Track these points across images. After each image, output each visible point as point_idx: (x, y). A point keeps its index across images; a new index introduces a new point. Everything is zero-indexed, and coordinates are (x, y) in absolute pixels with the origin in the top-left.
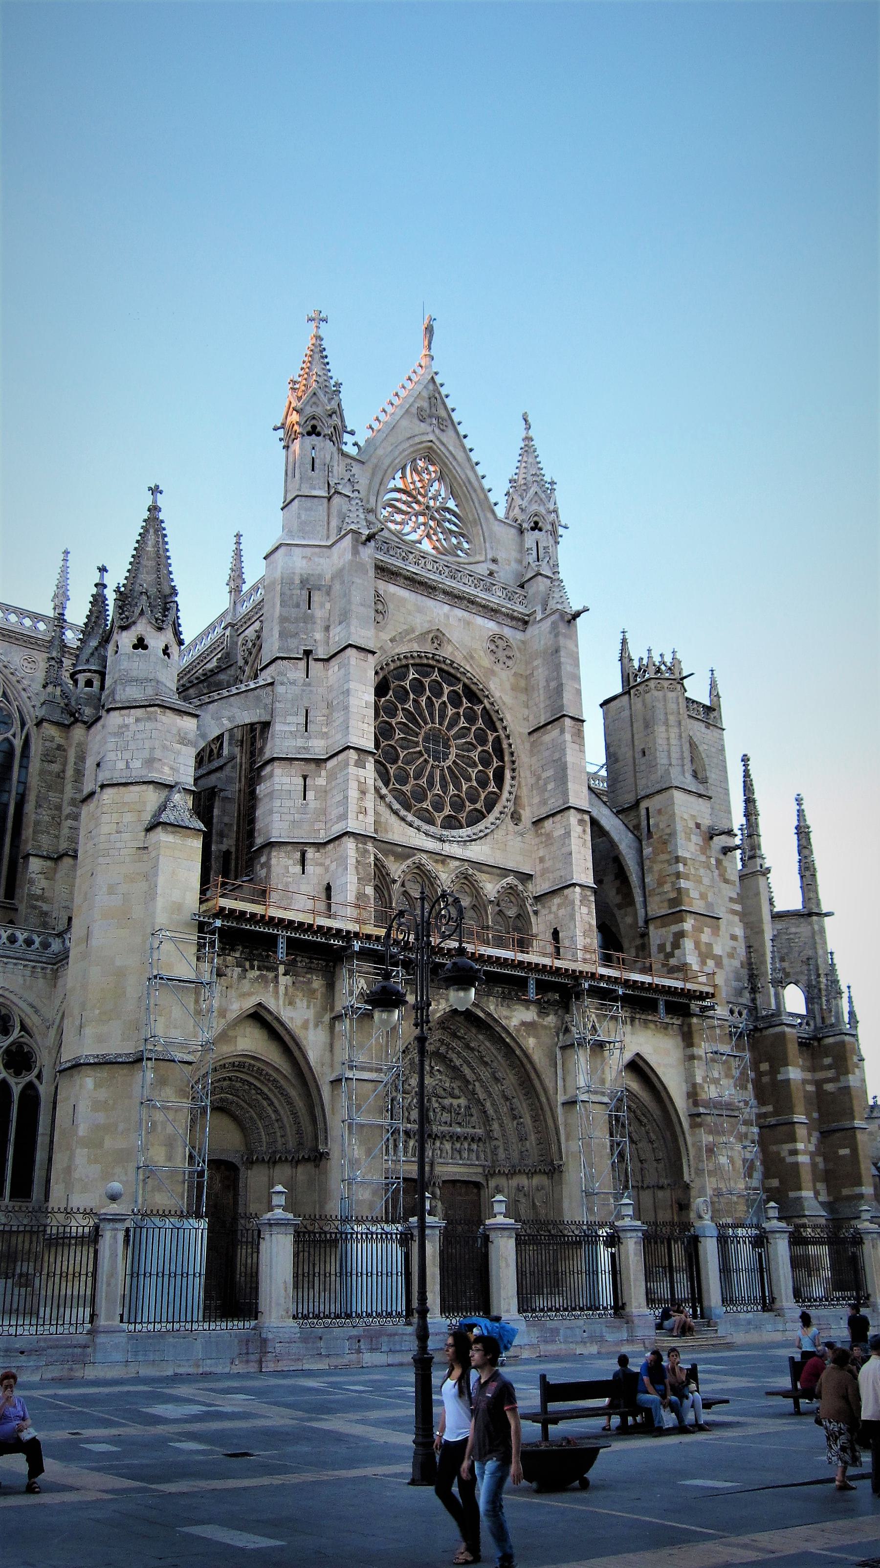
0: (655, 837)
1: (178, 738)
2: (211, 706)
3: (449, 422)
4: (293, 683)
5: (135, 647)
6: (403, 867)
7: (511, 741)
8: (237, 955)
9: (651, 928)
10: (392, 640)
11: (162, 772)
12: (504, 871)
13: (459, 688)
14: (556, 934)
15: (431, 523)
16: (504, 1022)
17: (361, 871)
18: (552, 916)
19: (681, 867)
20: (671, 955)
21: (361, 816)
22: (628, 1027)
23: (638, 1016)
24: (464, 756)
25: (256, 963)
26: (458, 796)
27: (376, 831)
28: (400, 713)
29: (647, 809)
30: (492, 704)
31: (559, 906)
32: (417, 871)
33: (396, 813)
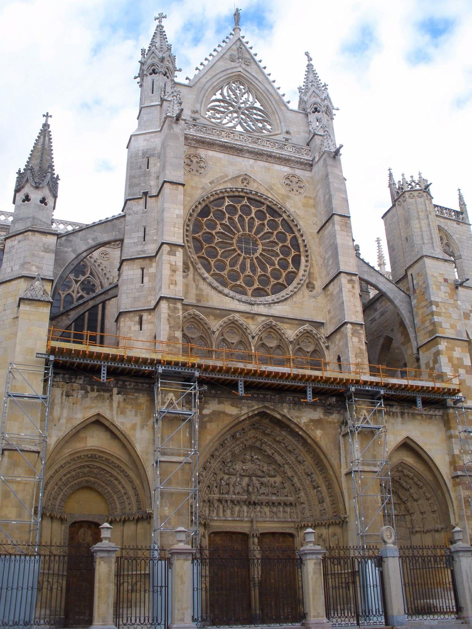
0: (417, 292)
1: (42, 249)
2: (80, 233)
3: (252, 60)
4: (136, 213)
5: (24, 201)
6: (221, 322)
7: (304, 238)
8: (81, 382)
9: (421, 353)
10: (210, 183)
11: (31, 270)
12: (301, 322)
13: (264, 208)
14: (339, 359)
15: (243, 117)
16: (295, 420)
17: (172, 322)
18: (336, 347)
19: (434, 308)
20: (433, 369)
21: (172, 287)
22: (399, 419)
23: (406, 411)
24: (269, 250)
25: (95, 387)
26: (265, 275)
27: (199, 301)
28: (219, 226)
29: (412, 275)
30: (289, 216)
31: (340, 340)
32: (234, 325)
33: (215, 288)
